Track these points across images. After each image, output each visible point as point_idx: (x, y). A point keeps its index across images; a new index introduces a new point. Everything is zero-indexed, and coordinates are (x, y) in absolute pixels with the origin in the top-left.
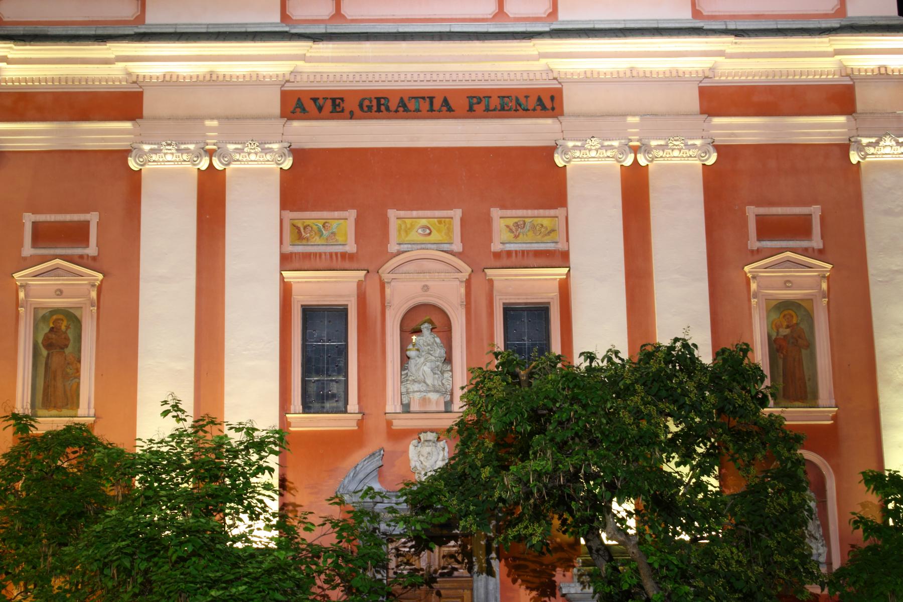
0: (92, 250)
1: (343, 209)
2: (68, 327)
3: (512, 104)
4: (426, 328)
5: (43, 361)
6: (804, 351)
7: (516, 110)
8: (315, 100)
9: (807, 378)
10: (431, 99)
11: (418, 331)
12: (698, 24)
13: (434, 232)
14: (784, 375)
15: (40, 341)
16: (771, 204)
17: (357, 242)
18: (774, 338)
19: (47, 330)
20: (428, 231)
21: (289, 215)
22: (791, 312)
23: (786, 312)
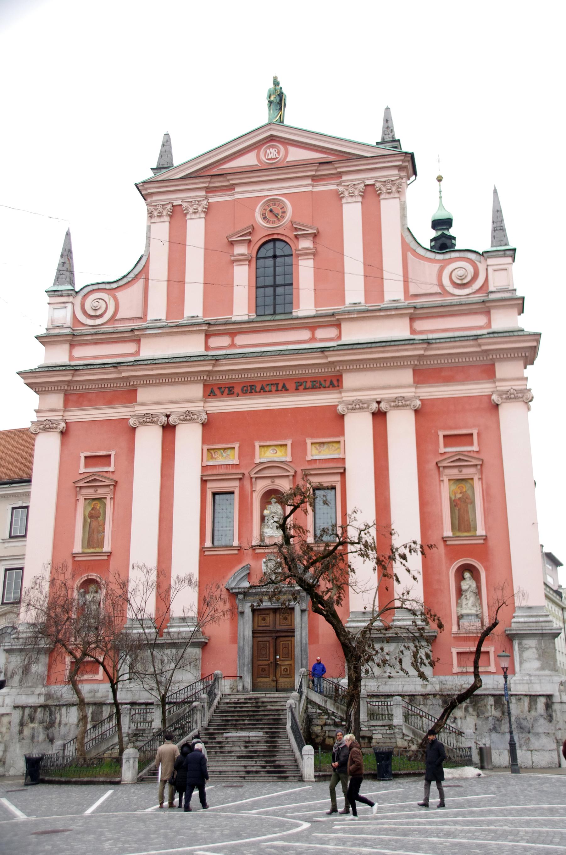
0: (111, 469)
1: (233, 442)
2: (100, 507)
3: (318, 385)
4: (274, 500)
5: (88, 524)
6: (469, 506)
7: (320, 388)
9: (471, 520)
10: (277, 385)
11: (270, 503)
12: (412, 337)
13: (278, 451)
14: (459, 519)
15: (87, 514)
16: (451, 428)
17: (239, 458)
18: (453, 498)
19: (90, 509)
20: (275, 451)
21: (206, 447)
22: (462, 485)
23: (460, 485)
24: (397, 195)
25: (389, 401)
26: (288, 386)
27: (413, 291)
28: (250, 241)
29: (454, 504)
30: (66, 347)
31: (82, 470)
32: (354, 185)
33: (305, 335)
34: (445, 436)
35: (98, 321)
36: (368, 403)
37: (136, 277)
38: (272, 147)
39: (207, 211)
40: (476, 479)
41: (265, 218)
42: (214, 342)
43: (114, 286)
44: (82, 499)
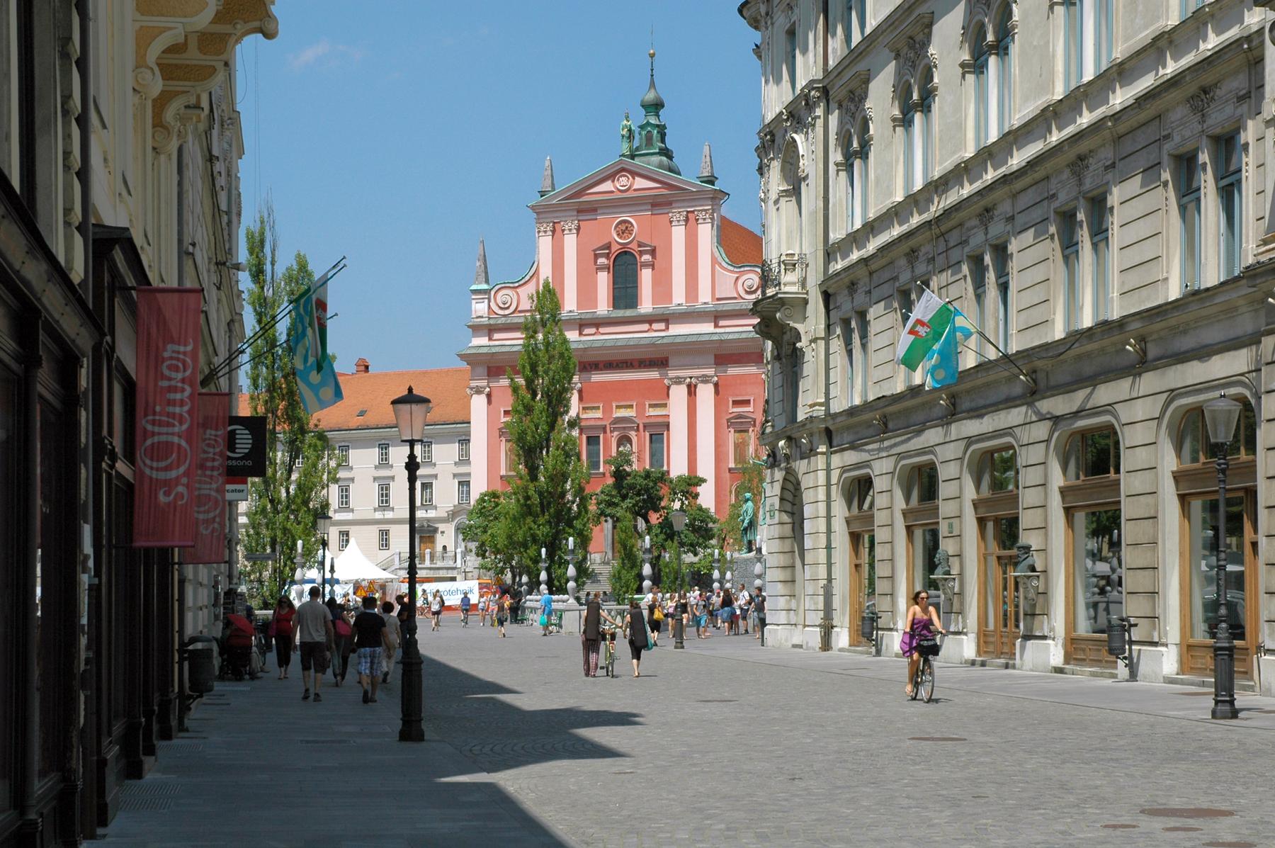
8: (589, 364)
24: (710, 221)
25: (697, 378)
26: (634, 364)
27: (717, 297)
28: (608, 254)
29: (737, 446)
30: (487, 331)
31: (503, 420)
32: (679, 212)
33: (646, 326)
34: (733, 401)
35: (507, 312)
36: (685, 378)
37: (531, 277)
38: (624, 176)
39: (578, 229)
40: (751, 430)
41: (618, 235)
42: (586, 331)
43: (517, 285)
44: (504, 439)
